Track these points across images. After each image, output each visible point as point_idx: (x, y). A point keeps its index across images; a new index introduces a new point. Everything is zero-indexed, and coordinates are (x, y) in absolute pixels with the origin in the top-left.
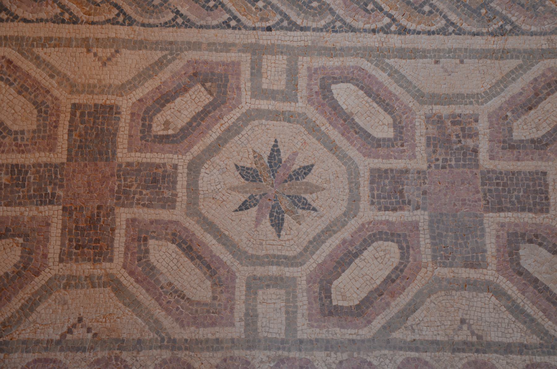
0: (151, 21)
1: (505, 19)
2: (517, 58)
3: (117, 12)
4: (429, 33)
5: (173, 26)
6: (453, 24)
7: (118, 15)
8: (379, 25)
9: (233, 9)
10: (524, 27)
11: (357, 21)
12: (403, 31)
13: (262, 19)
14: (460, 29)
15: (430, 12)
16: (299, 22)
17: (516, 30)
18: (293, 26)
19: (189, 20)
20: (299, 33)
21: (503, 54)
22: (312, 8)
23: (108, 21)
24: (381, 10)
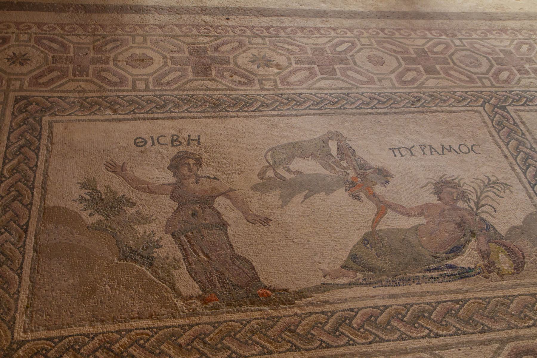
0: (310, 347)
1: (482, 324)
2: (496, 343)
3: (291, 345)
4: (451, 335)
5: (321, 348)
6: (459, 329)
7: (292, 346)
8: (424, 334)
9: (349, 334)
10: (493, 327)
11: (413, 333)
12: (437, 336)
13: (365, 339)
14: (464, 332)
15: (446, 325)
16: (384, 337)
17: (490, 330)
18: (382, 340)
19: (328, 344)
20: (386, 343)
21: (490, 342)
22: (388, 329)
23: (288, 350)
24: (423, 326)
